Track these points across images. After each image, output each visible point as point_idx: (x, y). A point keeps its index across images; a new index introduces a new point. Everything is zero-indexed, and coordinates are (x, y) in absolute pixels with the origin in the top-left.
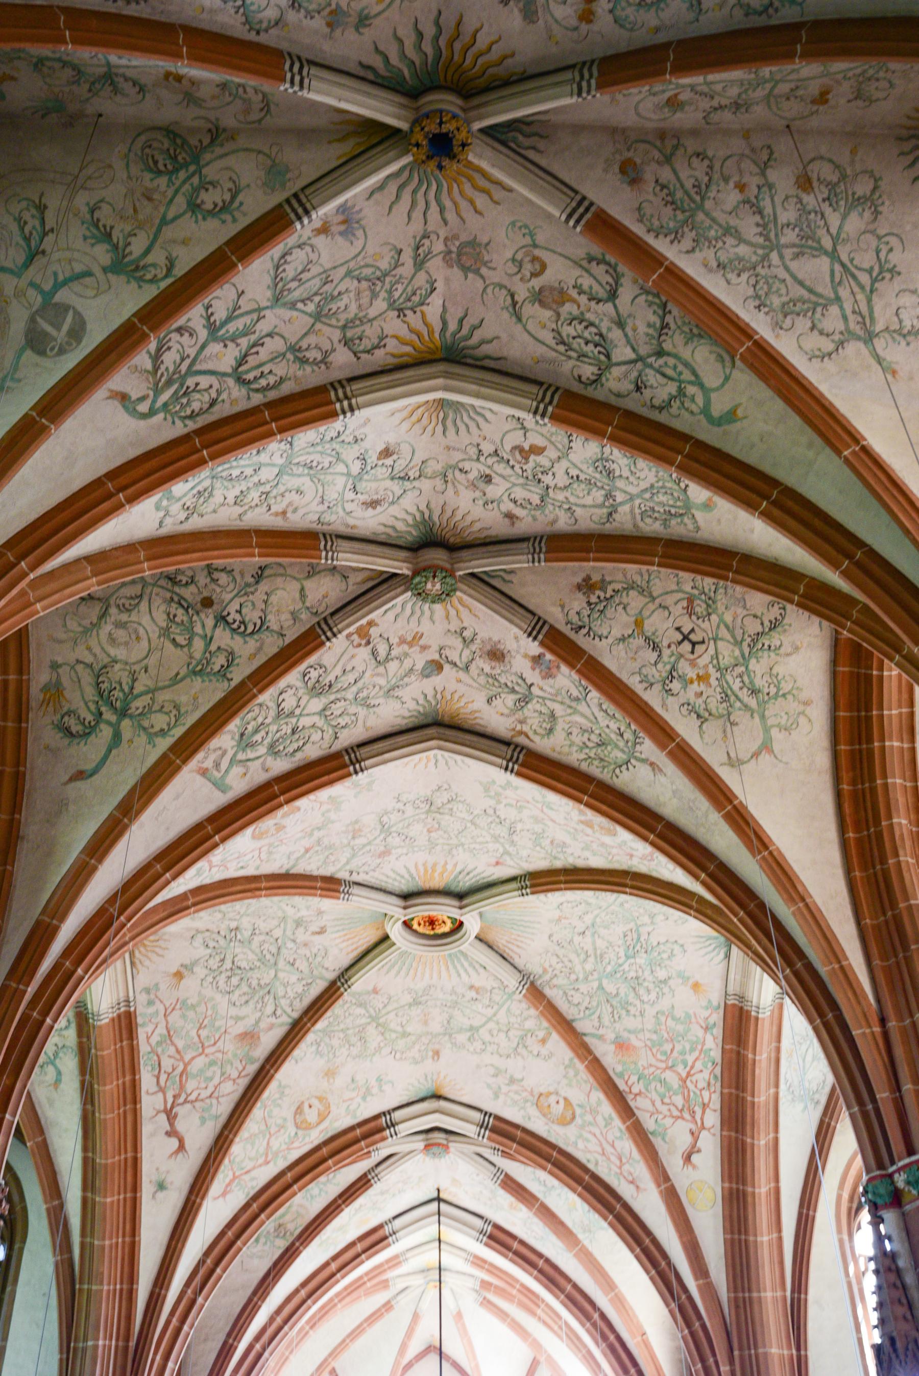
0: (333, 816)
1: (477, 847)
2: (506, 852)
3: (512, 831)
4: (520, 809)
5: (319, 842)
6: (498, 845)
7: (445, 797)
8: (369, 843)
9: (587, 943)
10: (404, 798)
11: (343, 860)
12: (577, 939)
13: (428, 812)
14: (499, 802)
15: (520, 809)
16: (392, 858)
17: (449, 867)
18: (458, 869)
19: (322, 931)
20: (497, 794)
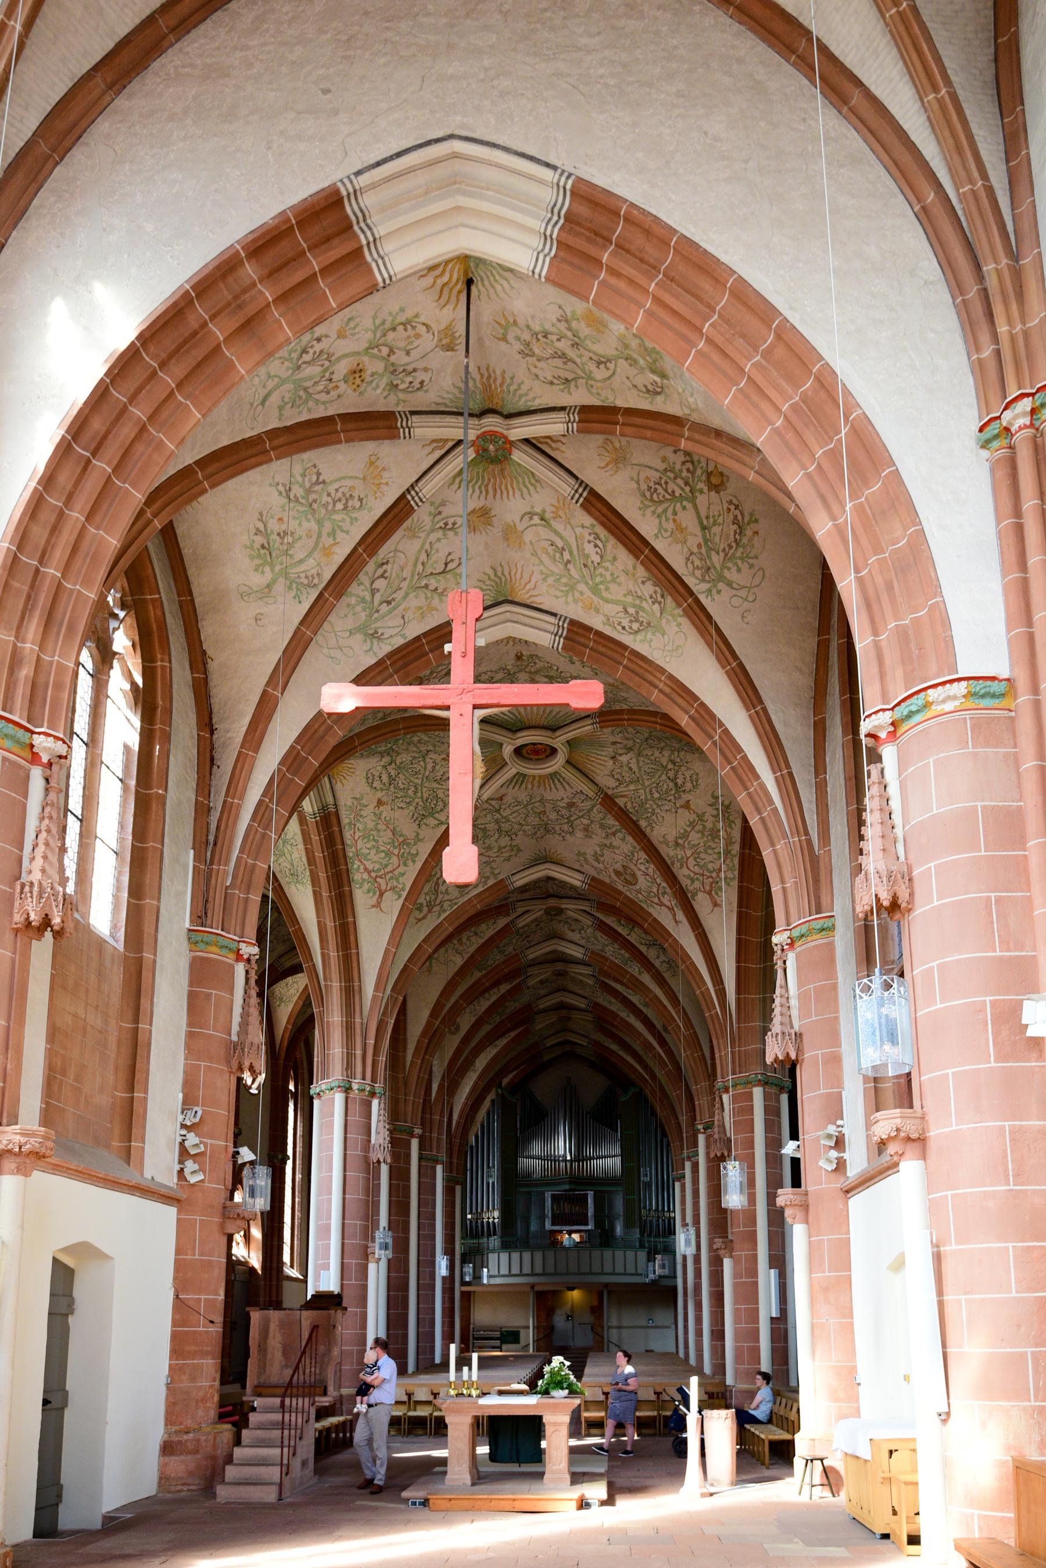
0: (598, 849)
1: (516, 808)
2: (498, 811)
3: (499, 830)
4: (500, 848)
5: (607, 836)
6: (504, 814)
7: (538, 835)
8: (580, 817)
9: (423, 748)
10: (561, 838)
11: (595, 810)
12: (431, 748)
13: (547, 824)
14: (511, 845)
15: (500, 848)
16: (566, 800)
17: (530, 786)
18: (524, 786)
19: (614, 743)
20: (512, 850)
